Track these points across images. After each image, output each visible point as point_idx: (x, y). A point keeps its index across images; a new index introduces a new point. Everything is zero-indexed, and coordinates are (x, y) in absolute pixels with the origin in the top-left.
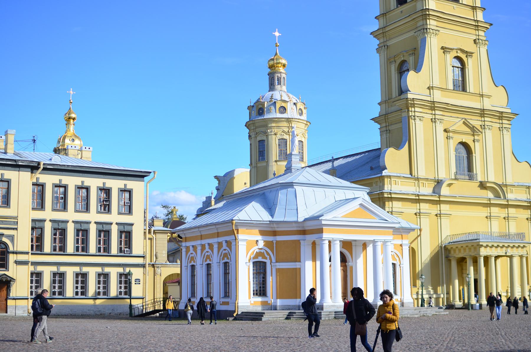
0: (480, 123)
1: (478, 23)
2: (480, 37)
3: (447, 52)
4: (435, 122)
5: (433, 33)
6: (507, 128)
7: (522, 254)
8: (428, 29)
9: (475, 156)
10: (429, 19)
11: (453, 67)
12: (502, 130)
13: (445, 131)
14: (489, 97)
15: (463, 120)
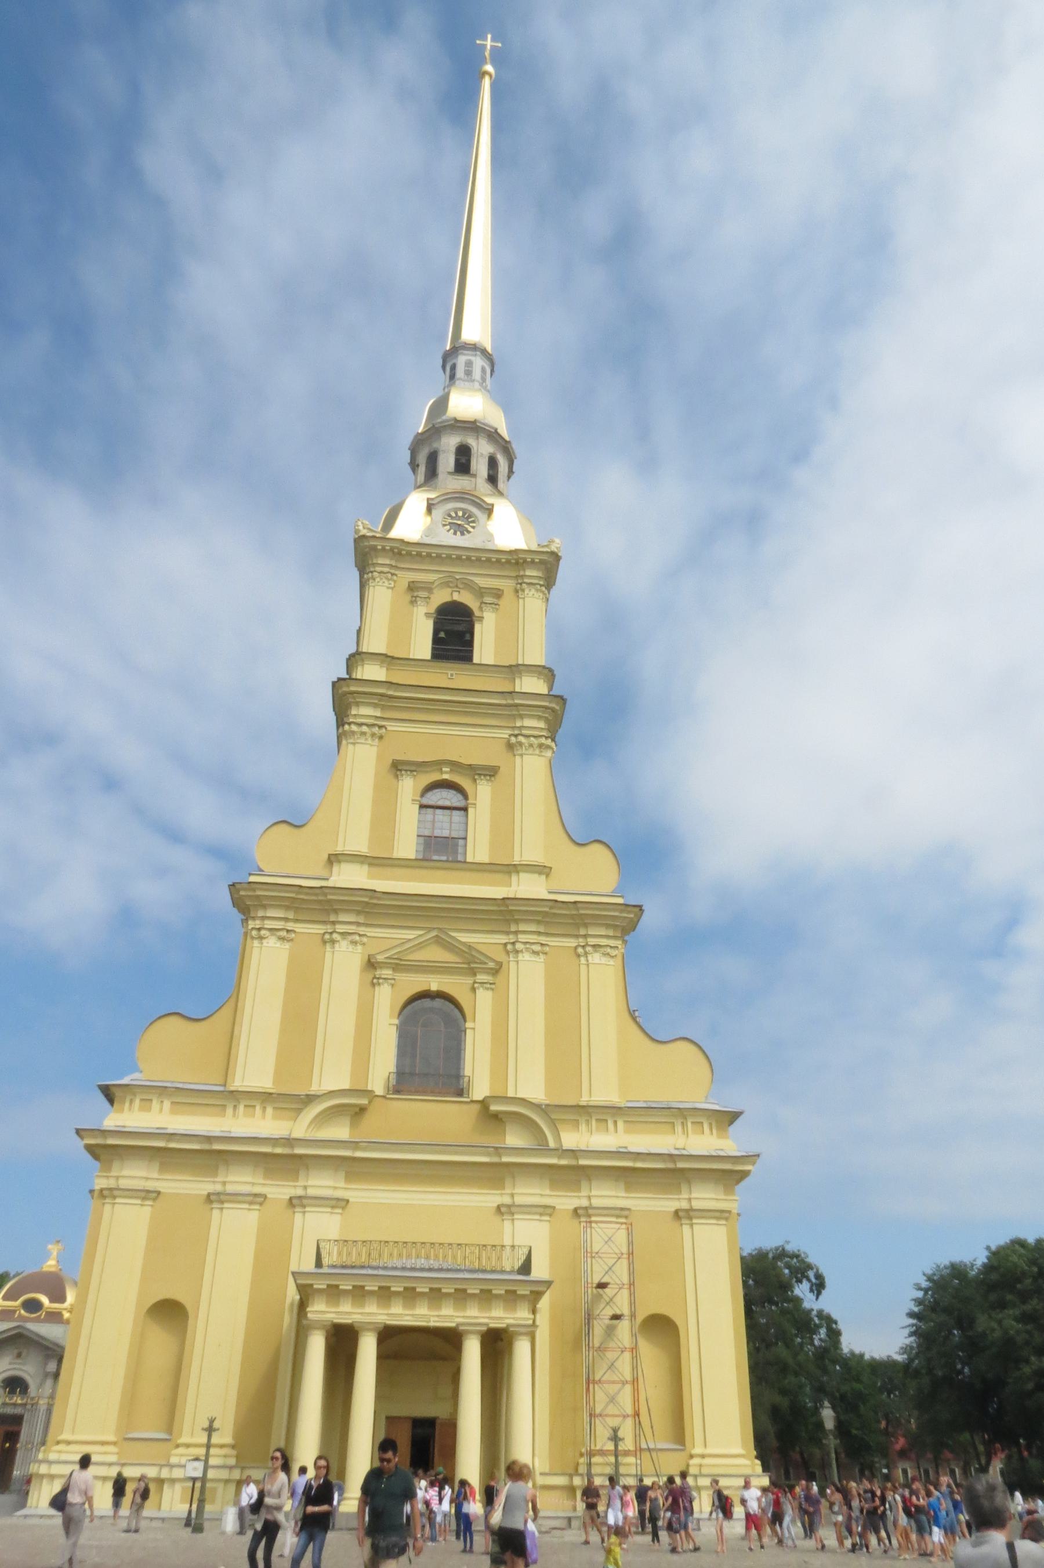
0: (502, 939)
1: (513, 699)
2: (524, 732)
3: (403, 772)
5: (364, 734)
6: (600, 946)
7: (511, 1321)
8: (347, 727)
9: (474, 1029)
10: (358, 704)
11: (422, 807)
12: (586, 954)
13: (371, 964)
14: (543, 870)
15: (434, 934)
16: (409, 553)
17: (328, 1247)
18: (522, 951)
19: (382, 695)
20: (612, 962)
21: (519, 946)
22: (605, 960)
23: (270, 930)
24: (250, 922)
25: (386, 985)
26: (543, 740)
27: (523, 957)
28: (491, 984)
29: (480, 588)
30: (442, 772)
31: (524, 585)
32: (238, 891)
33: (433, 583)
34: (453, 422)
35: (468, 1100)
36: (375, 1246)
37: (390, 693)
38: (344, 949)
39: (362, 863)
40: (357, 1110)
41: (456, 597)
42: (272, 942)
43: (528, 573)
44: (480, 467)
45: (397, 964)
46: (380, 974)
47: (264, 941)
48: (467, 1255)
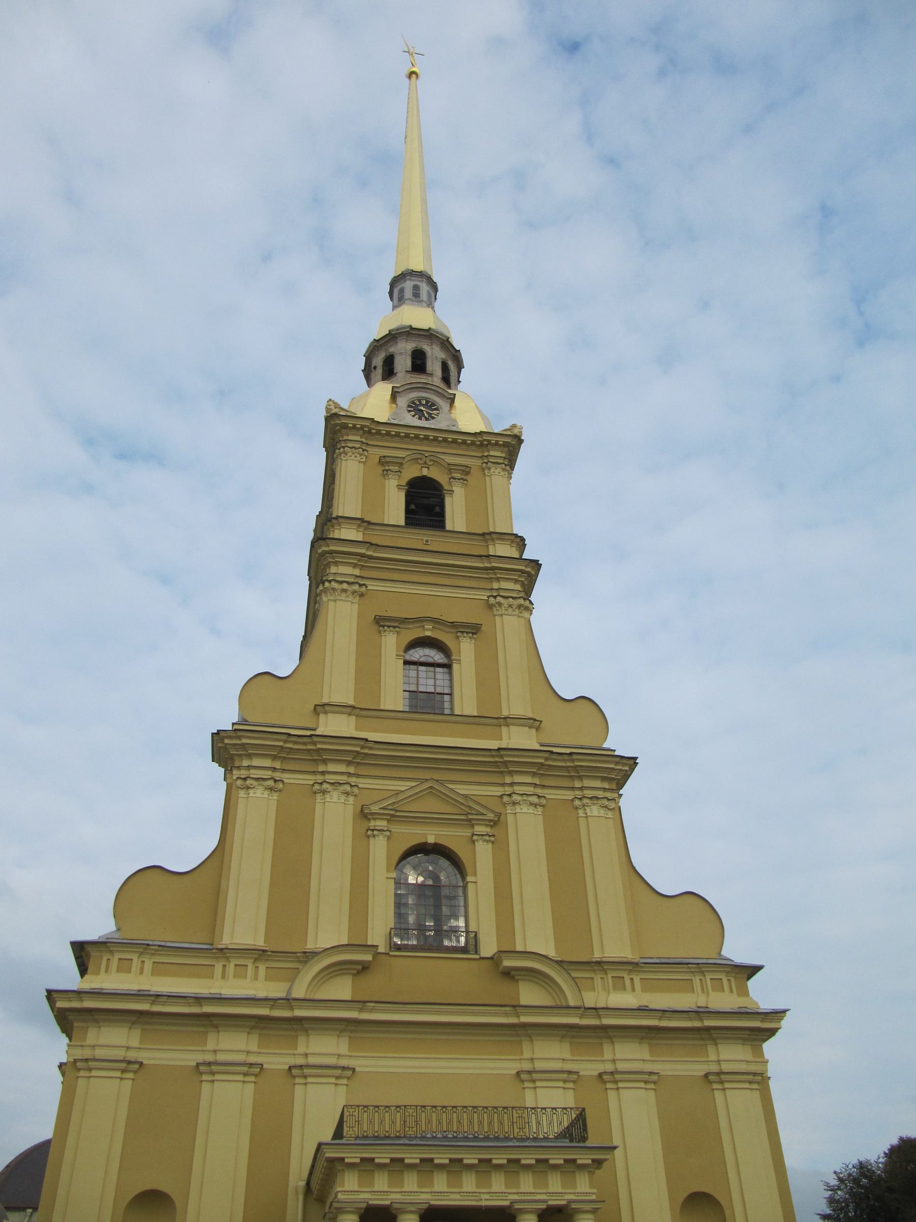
0: (498, 790)
3: (386, 628)
4: (324, 792)
6: (597, 798)
8: (327, 584)
10: (336, 563)
13: (364, 814)
14: (533, 723)
16: (378, 433)
17: (356, 1114)
18: (519, 803)
19: (363, 555)
20: (610, 814)
21: (516, 798)
22: (602, 812)
23: (257, 779)
24: (235, 772)
25: (381, 837)
26: (521, 601)
27: (521, 809)
28: (490, 836)
29: (448, 464)
30: (424, 629)
31: (489, 464)
32: (223, 738)
33: (404, 458)
34: (408, 329)
35: (477, 957)
36: (411, 1111)
37: (370, 553)
38: (335, 799)
39: (350, 714)
40: (360, 967)
41: (425, 472)
42: (259, 793)
43: (492, 453)
44: (434, 366)
45: (392, 816)
46: (374, 826)
47: (251, 791)
48: (515, 1121)
